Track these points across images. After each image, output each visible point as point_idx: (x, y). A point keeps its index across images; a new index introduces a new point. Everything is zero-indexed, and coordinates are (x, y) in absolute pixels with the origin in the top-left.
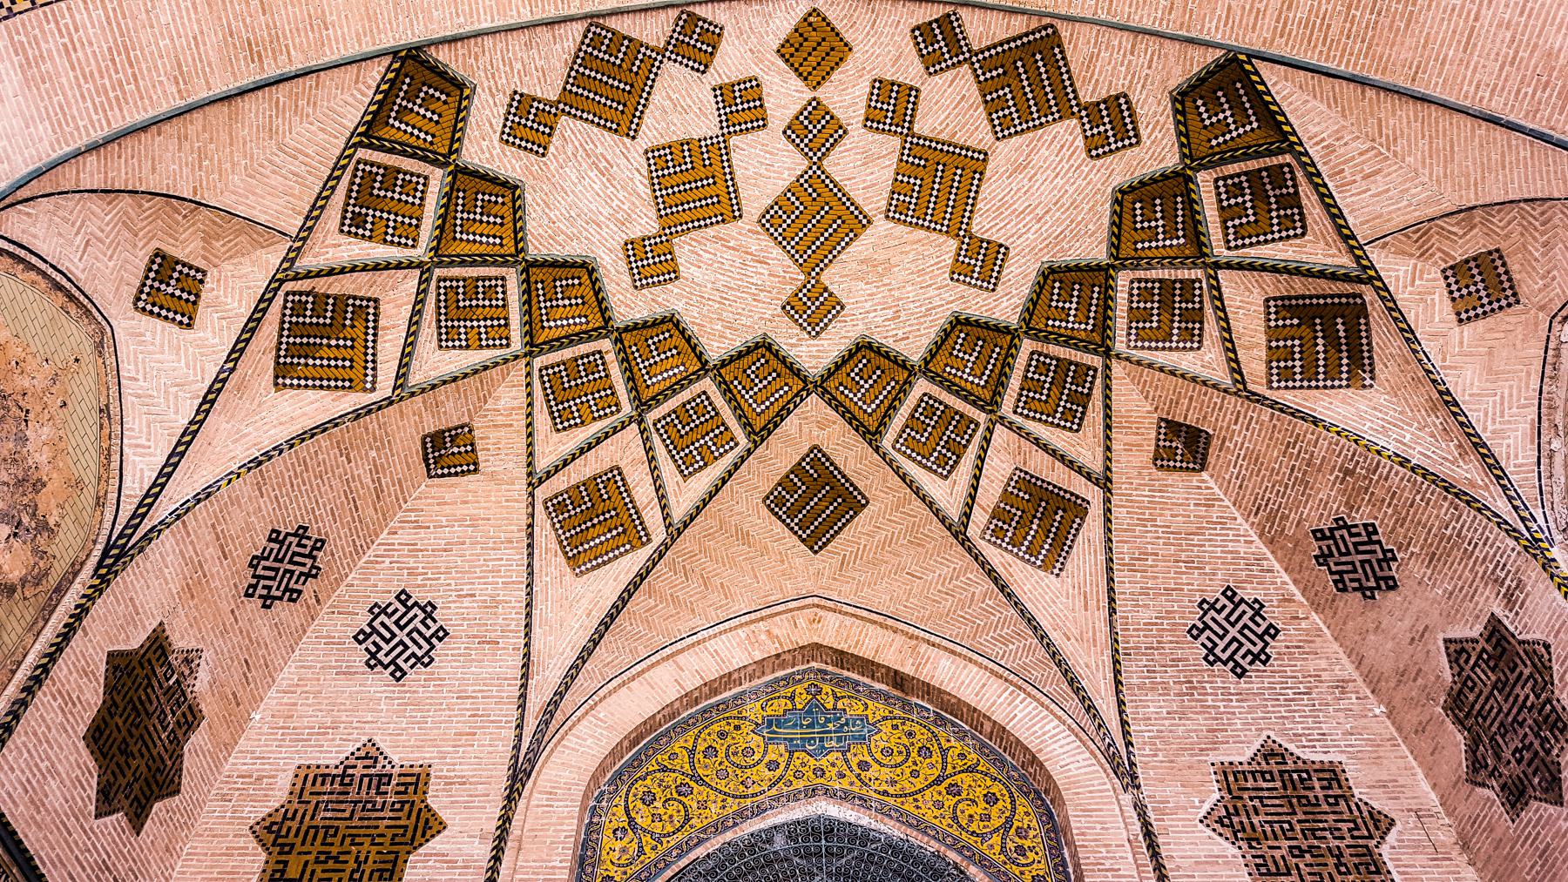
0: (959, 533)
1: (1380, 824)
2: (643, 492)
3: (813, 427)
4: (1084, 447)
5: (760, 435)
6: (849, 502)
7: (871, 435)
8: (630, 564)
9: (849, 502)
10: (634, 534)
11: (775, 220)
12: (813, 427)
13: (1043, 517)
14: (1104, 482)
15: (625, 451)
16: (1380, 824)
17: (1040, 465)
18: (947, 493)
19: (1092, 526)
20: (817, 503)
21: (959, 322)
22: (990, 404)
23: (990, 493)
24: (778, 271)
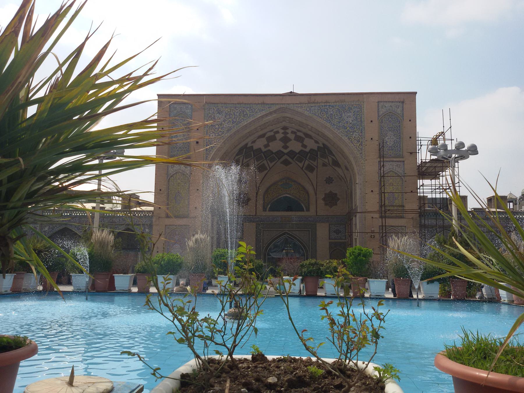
0: (302, 168)
1: (338, 199)
2: (267, 165)
3: (286, 157)
4: (315, 163)
5: (279, 159)
6: (290, 163)
7: (292, 159)
8: (266, 171)
9: (290, 163)
10: (267, 169)
11: (281, 140)
12: (286, 157)
13: (311, 169)
14: (317, 167)
15: (265, 162)
16: (338, 199)
17: (310, 164)
18: (301, 165)
19: (315, 171)
20: (286, 163)
21: (302, 150)
22: (306, 158)
23: (305, 165)
24: (282, 144)
